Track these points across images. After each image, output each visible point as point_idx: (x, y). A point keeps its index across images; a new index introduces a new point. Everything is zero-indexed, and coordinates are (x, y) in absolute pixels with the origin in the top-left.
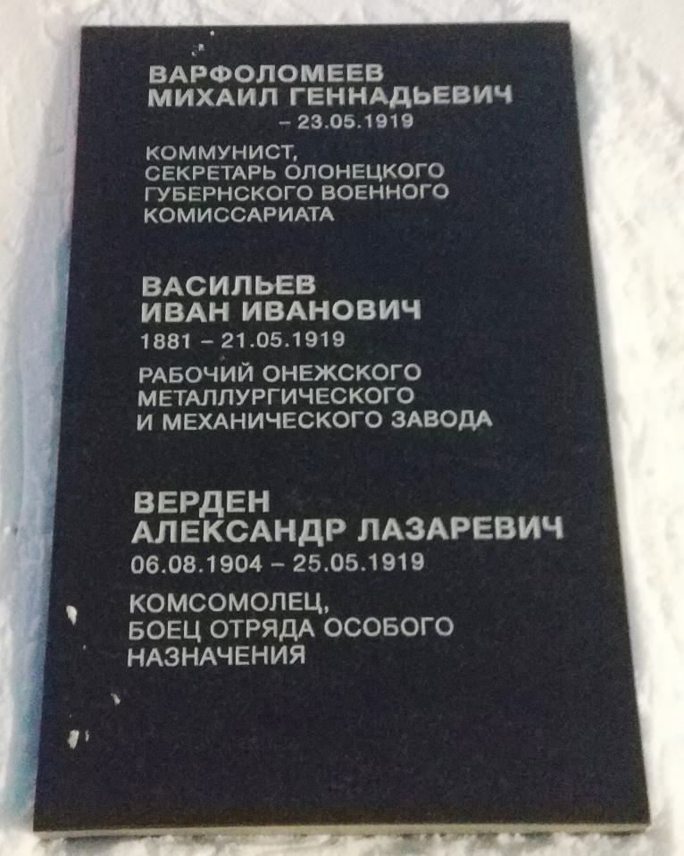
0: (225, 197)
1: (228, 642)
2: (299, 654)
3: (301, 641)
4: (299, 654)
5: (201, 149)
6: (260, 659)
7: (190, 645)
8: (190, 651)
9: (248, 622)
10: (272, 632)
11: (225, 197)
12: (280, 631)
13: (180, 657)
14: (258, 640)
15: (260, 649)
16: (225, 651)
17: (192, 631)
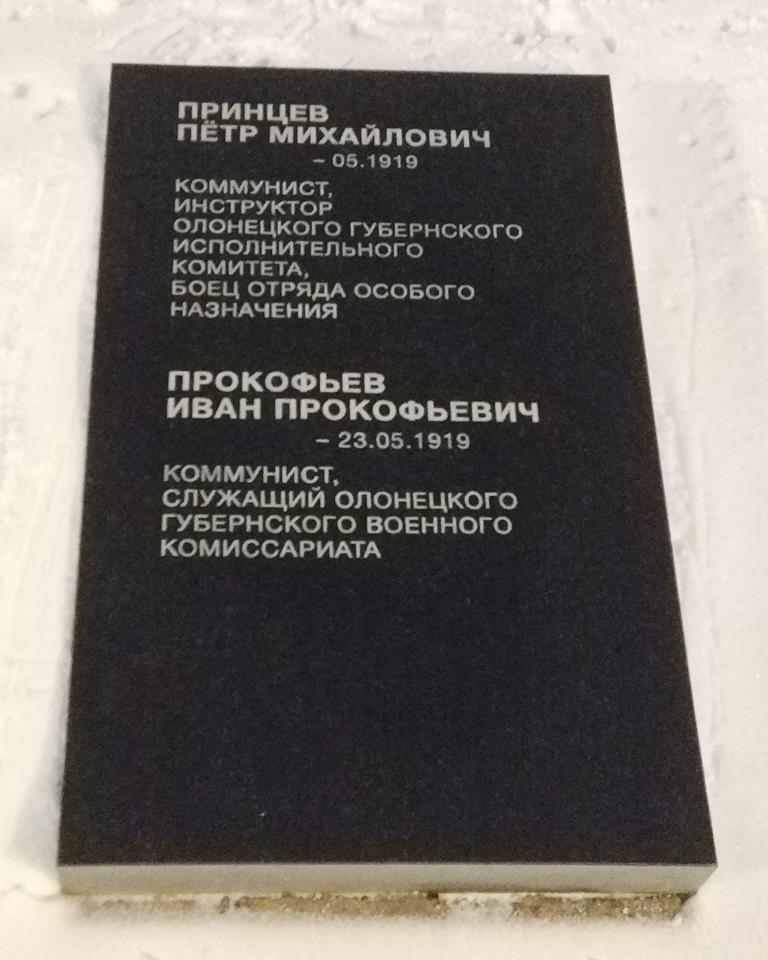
0: (255, 528)
1: (266, 299)
2: (332, 310)
3: (332, 301)
4: (332, 310)
5: (228, 469)
6: (295, 315)
7: (230, 301)
8: (229, 305)
9: (284, 284)
10: (305, 293)
11: (255, 528)
12: (313, 292)
13: (216, 310)
14: (293, 298)
15: (295, 306)
16: (262, 306)
17: (230, 289)
